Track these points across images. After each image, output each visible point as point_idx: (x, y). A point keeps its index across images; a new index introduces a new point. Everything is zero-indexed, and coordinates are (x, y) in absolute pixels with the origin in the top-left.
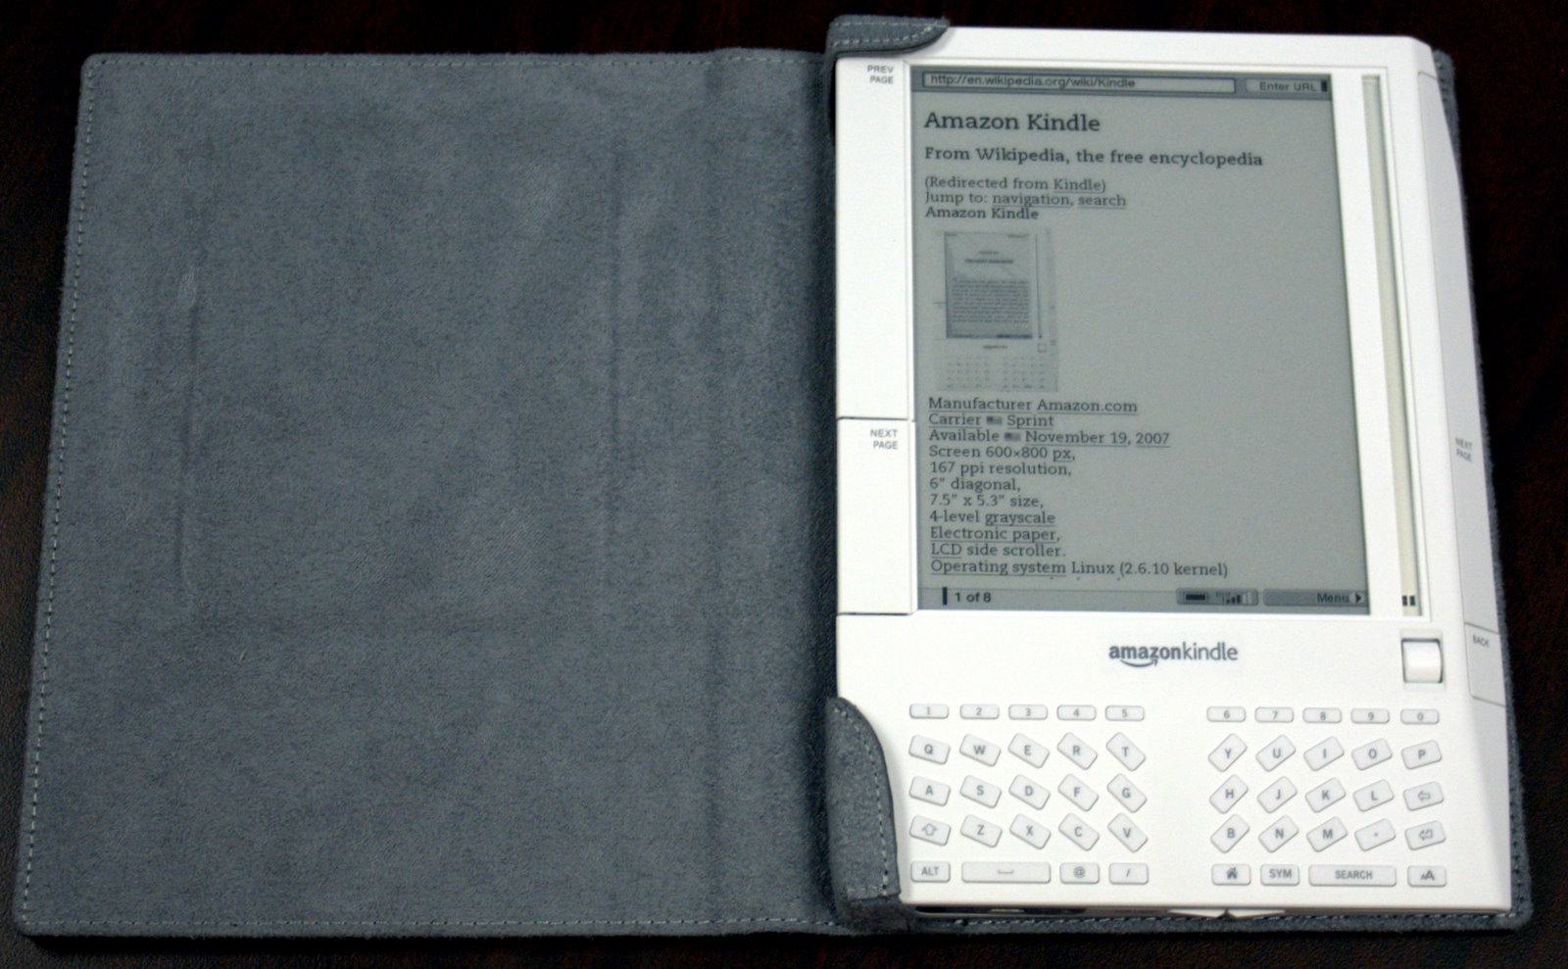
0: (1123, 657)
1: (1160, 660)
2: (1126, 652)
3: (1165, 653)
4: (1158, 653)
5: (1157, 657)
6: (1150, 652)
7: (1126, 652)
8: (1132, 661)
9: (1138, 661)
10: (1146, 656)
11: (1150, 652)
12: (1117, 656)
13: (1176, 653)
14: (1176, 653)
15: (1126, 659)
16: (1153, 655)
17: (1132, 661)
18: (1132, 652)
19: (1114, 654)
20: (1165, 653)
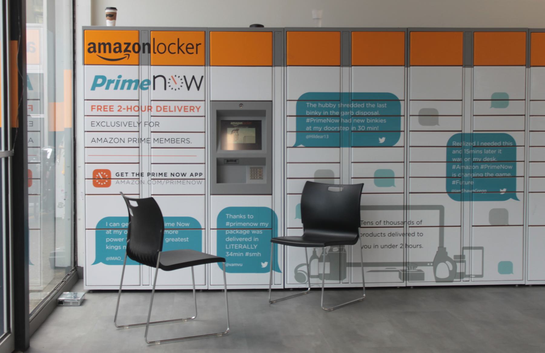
0: (100, 52)
1: (132, 54)
2: (102, 46)
3: (136, 49)
4: (130, 48)
5: (130, 51)
6: (124, 47)
7: (102, 46)
8: (107, 55)
9: (113, 56)
10: (120, 51)
11: (124, 47)
12: (95, 51)
13: (146, 47)
14: (146, 47)
15: (102, 54)
16: (126, 50)
17: (107, 55)
18: (107, 46)
19: (92, 50)
20: (137, 50)
